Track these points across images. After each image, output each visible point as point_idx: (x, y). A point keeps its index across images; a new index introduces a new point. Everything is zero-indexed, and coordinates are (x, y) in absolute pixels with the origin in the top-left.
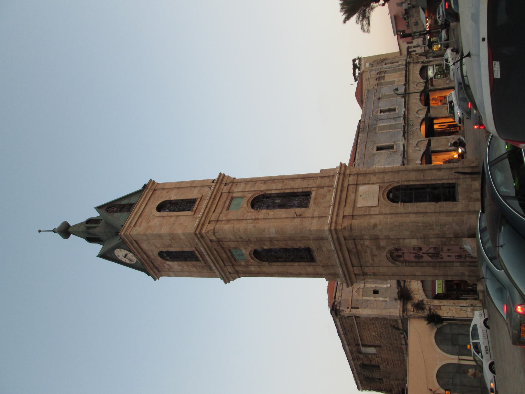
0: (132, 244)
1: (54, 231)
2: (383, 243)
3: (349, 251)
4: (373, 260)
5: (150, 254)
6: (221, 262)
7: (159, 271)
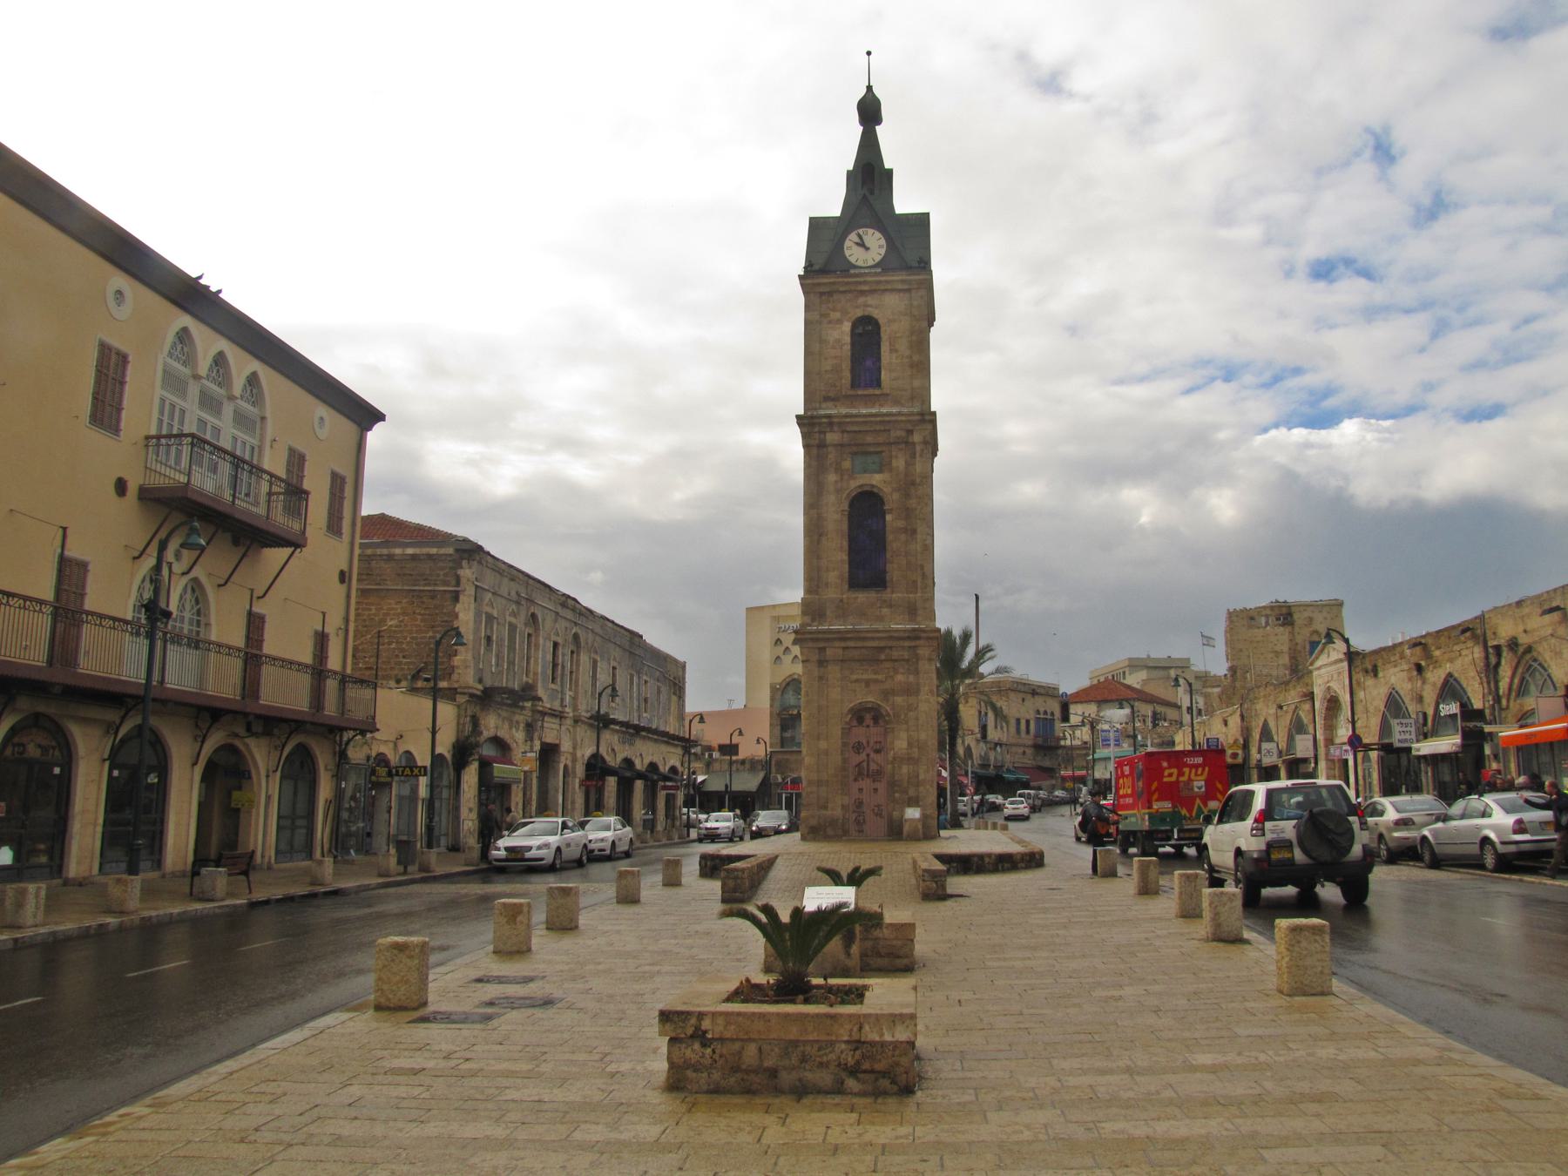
0: (903, 281)
1: (869, 88)
2: (899, 700)
3: (881, 649)
4: (857, 681)
5: (870, 300)
6: (856, 428)
7: (822, 294)
